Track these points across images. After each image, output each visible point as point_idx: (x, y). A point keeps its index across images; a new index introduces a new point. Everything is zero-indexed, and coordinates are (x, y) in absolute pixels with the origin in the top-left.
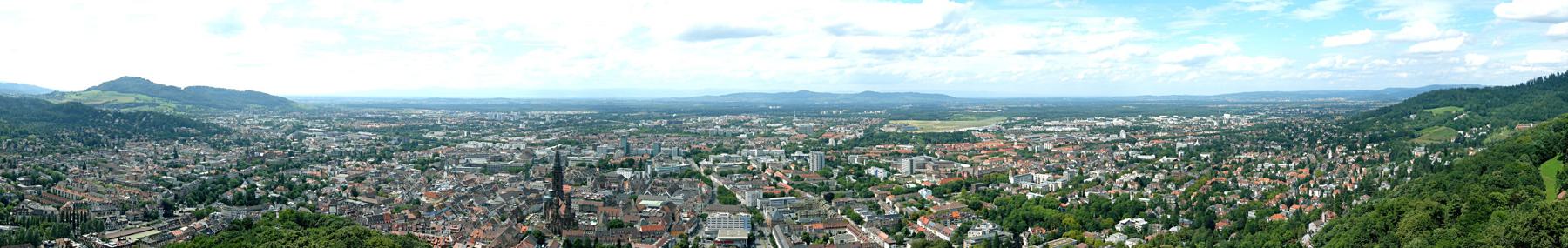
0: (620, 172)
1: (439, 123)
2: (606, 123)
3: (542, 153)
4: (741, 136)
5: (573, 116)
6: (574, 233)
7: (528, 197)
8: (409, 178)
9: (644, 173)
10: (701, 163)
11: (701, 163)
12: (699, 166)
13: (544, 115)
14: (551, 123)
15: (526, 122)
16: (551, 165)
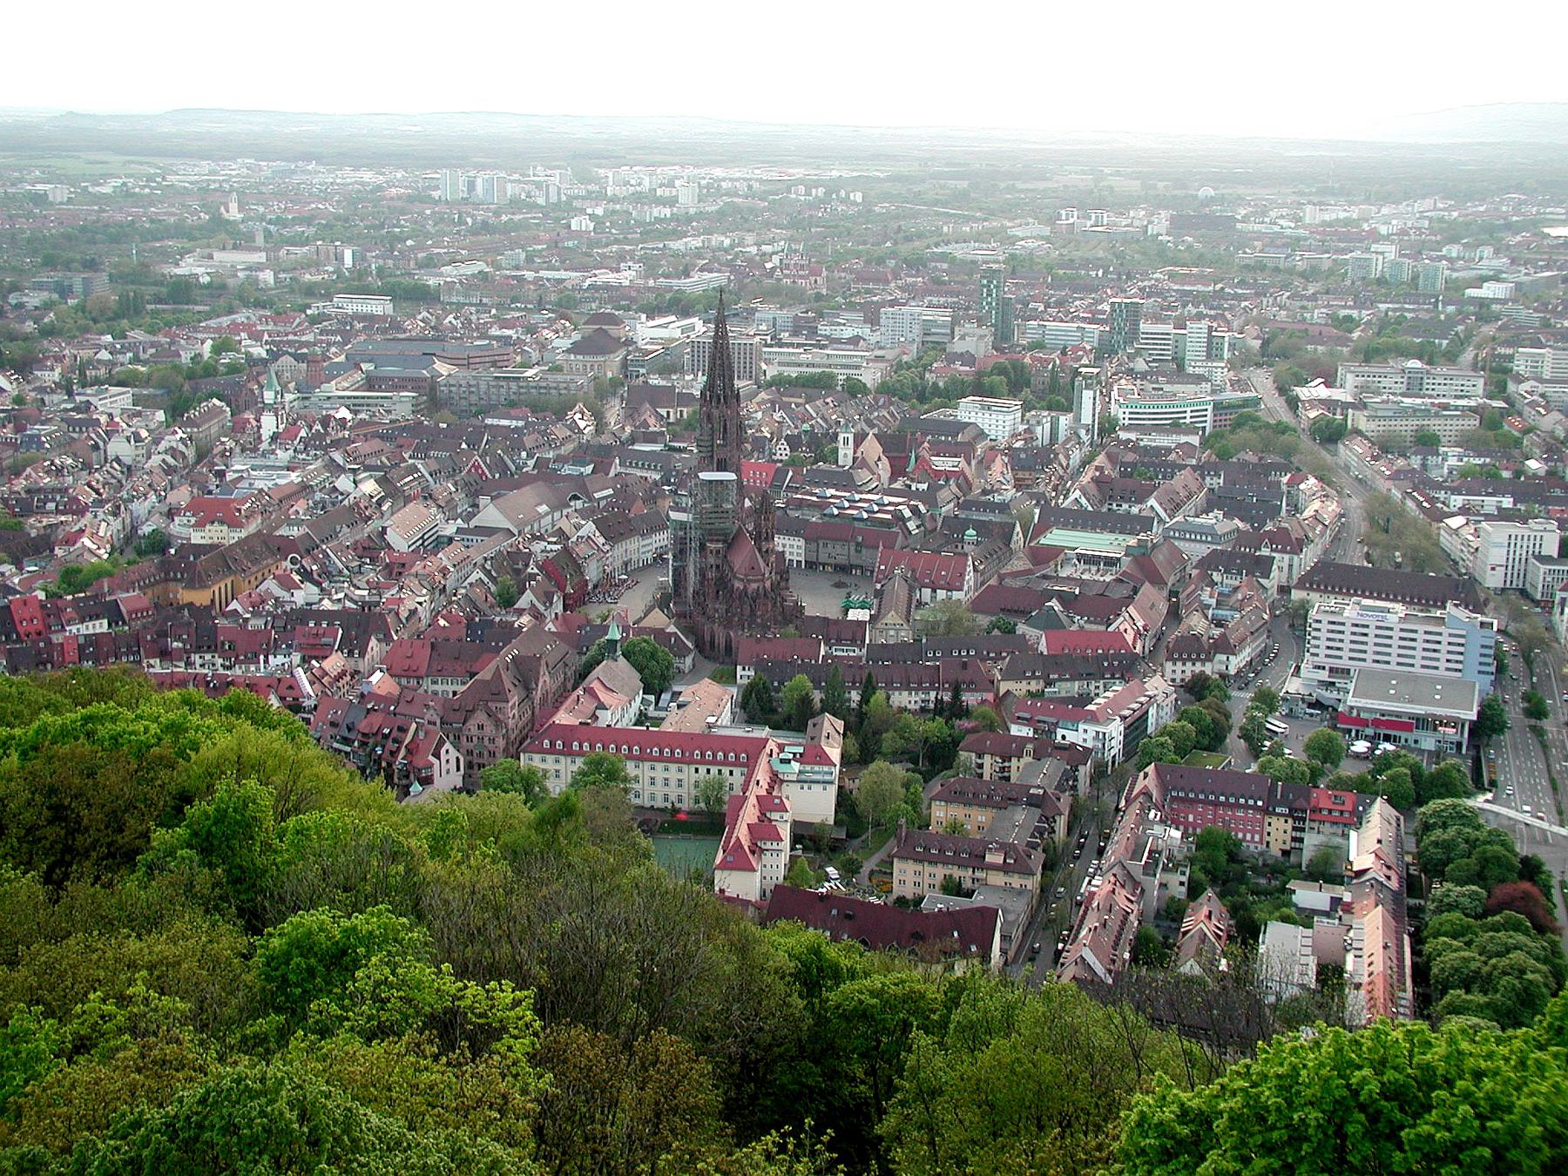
0: (968, 411)
1: (233, 213)
4: (1488, 291)
8: (119, 447)
9: (1065, 421)
10: (1303, 393)
11: (1303, 393)
12: (1293, 404)
13: (671, 184)
14: (700, 216)
16: (696, 383)
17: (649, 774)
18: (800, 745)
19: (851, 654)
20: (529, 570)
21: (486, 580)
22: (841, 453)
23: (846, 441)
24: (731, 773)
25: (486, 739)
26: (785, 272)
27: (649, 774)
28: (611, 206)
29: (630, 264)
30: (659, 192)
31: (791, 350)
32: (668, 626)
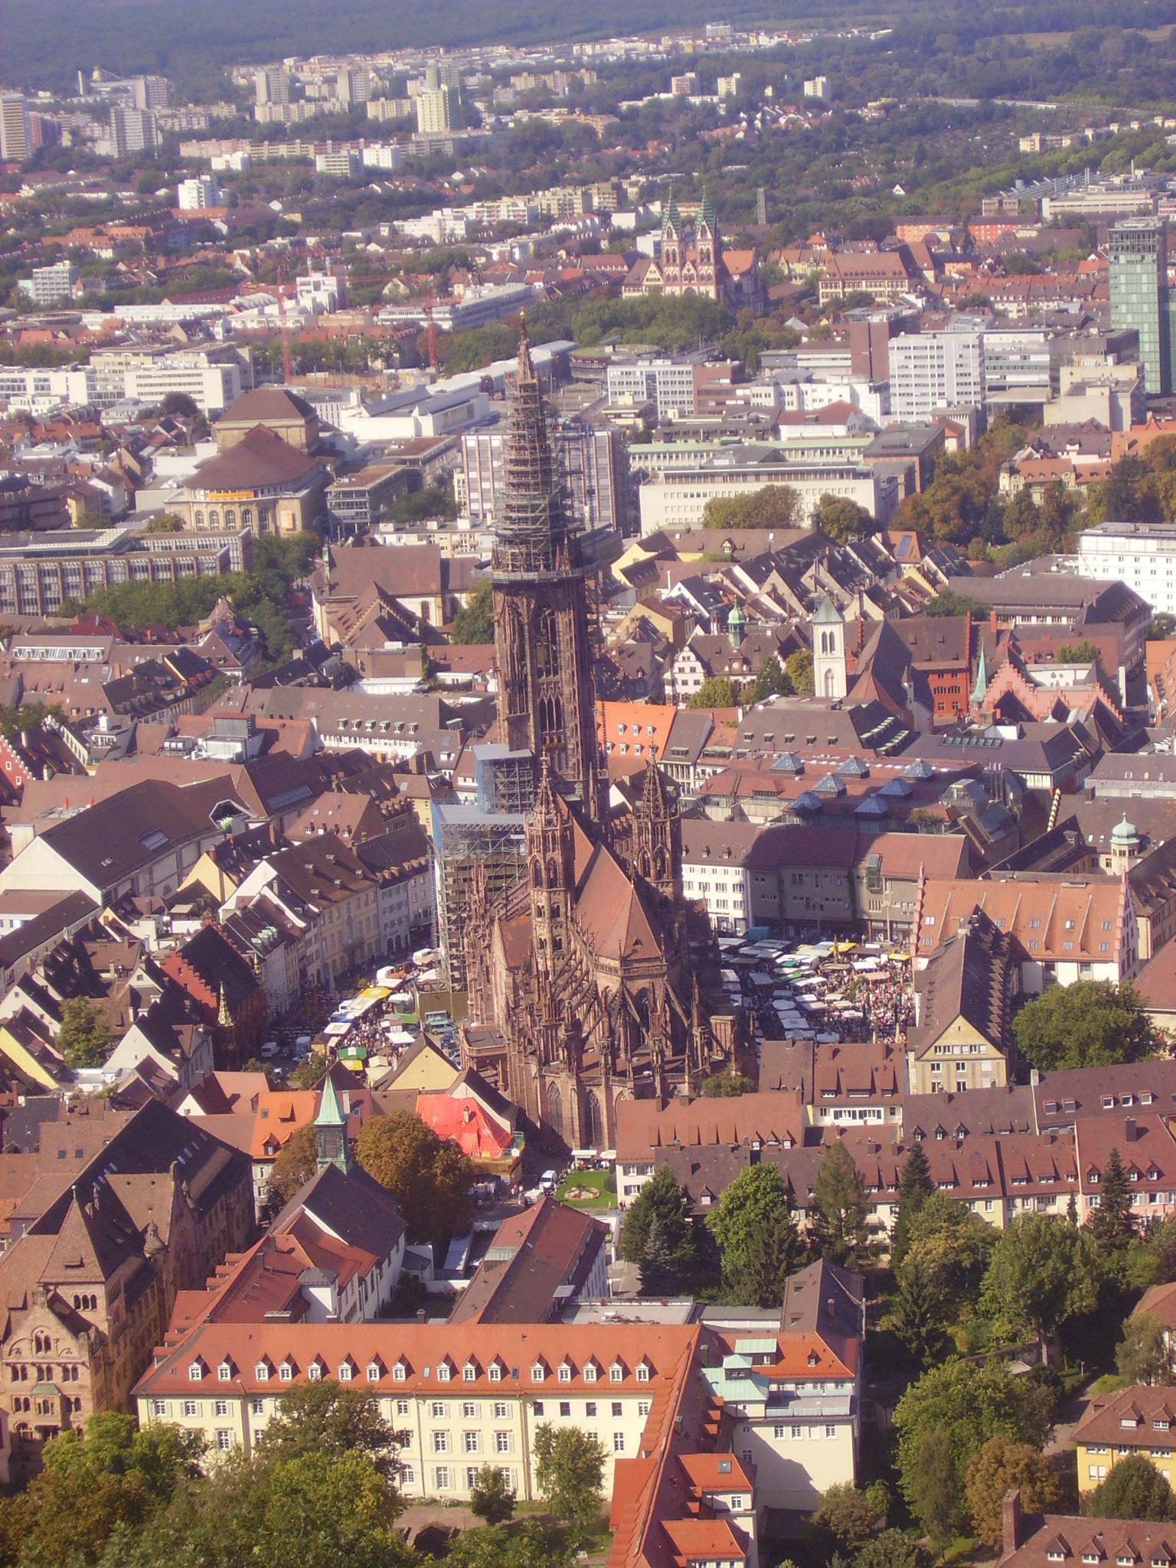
2: (961, 120)
3: (397, 429)
5: (658, 74)
6: (638, 539)
7: (301, 831)
14: (467, 151)
15: (230, 158)
17: (432, 1424)
18: (768, 1333)
19: (872, 1121)
20: (133, 982)
21: (37, 1010)
22: (819, 667)
23: (828, 643)
24: (617, 1410)
25: (58, 1372)
26: (671, 270)
27: (432, 1424)
28: (266, 151)
29: (316, 277)
30: (373, 111)
31: (692, 444)
32: (455, 1085)
